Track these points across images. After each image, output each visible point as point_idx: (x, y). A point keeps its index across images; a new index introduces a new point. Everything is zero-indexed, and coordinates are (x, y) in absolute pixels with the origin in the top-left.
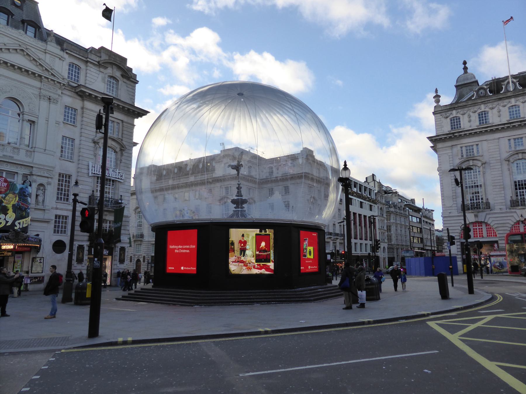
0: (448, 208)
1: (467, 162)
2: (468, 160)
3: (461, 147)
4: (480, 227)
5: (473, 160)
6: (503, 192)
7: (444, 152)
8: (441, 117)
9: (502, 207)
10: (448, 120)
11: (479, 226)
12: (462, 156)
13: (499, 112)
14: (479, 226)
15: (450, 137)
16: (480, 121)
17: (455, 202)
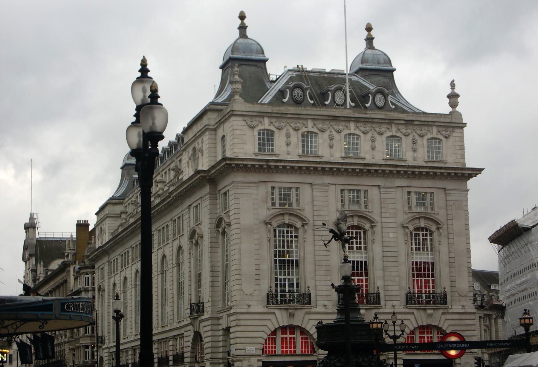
0: (246, 297)
1: (281, 218)
2: (283, 214)
3: (273, 188)
4: (292, 336)
5: (290, 214)
6: (329, 277)
7: (246, 191)
8: (244, 123)
9: (326, 303)
10: (256, 133)
11: (290, 334)
12: (273, 204)
13: (331, 139)
14: (290, 334)
15: (261, 166)
16: (303, 146)
17: (258, 287)
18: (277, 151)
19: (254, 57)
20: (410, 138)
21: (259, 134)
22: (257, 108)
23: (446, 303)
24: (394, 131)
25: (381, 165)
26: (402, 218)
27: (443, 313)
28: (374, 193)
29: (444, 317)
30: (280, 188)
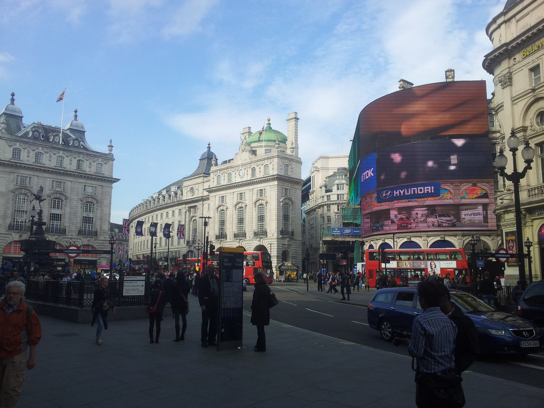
3: (18, 176)
10: (12, 149)
12: (17, 183)
16: (36, 158)
17: (4, 222)
18: (21, 159)
19: (16, 114)
20: (89, 162)
21: (13, 150)
22: (14, 138)
23: (97, 236)
24: (81, 157)
25: (73, 172)
26: (81, 196)
27: (95, 240)
28: (68, 184)
29: (95, 242)
30: (21, 176)
